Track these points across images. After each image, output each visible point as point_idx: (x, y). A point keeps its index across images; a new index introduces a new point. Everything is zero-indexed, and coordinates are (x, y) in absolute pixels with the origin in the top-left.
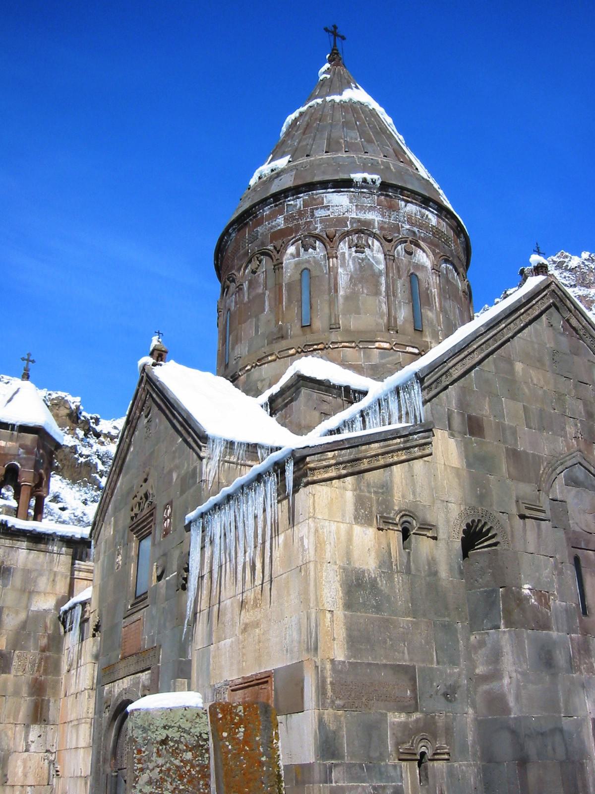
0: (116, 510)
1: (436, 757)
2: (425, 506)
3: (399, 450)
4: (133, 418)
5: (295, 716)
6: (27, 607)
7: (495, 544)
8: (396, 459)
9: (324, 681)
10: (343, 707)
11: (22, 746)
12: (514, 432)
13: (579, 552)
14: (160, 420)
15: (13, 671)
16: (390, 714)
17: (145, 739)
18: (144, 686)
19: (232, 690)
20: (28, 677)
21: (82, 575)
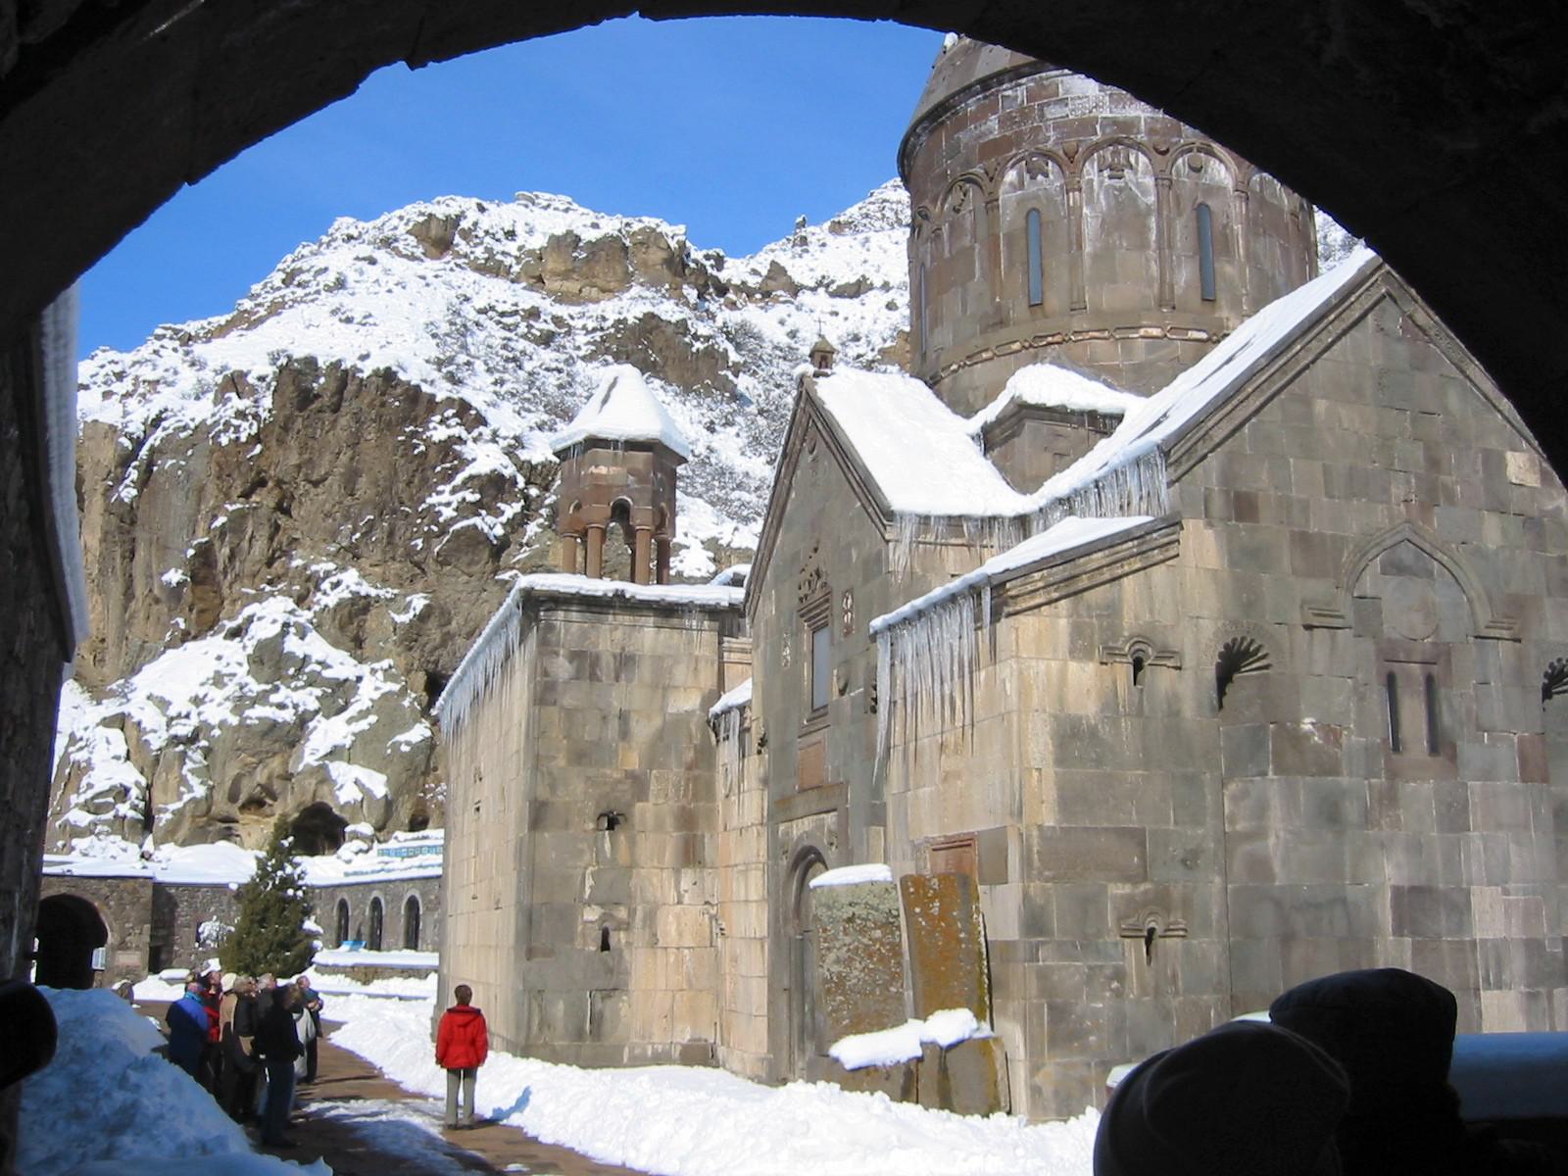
0: (777, 579)
2: (1165, 627)
3: (1132, 556)
4: (792, 449)
5: (1000, 888)
6: (663, 709)
7: (1266, 667)
8: (1127, 569)
9: (1029, 850)
11: (672, 896)
12: (1305, 507)
13: (1396, 667)
14: (830, 463)
17: (830, 917)
18: (830, 831)
19: (934, 850)
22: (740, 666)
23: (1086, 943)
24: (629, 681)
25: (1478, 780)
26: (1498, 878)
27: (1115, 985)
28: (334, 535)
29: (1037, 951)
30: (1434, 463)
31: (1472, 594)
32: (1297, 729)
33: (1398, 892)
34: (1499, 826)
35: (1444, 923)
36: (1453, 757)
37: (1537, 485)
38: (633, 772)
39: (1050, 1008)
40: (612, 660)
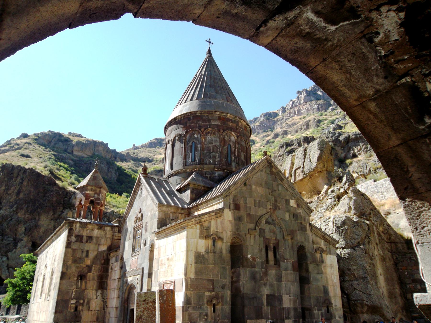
6: (98, 250)
11: (95, 297)
12: (250, 208)
15: (92, 272)
20: (97, 273)
21: (116, 238)
23: (199, 307)
24: (90, 243)
26: (288, 294)
27: (205, 317)
28: (12, 207)
32: (247, 257)
33: (267, 296)
34: (288, 281)
35: (277, 303)
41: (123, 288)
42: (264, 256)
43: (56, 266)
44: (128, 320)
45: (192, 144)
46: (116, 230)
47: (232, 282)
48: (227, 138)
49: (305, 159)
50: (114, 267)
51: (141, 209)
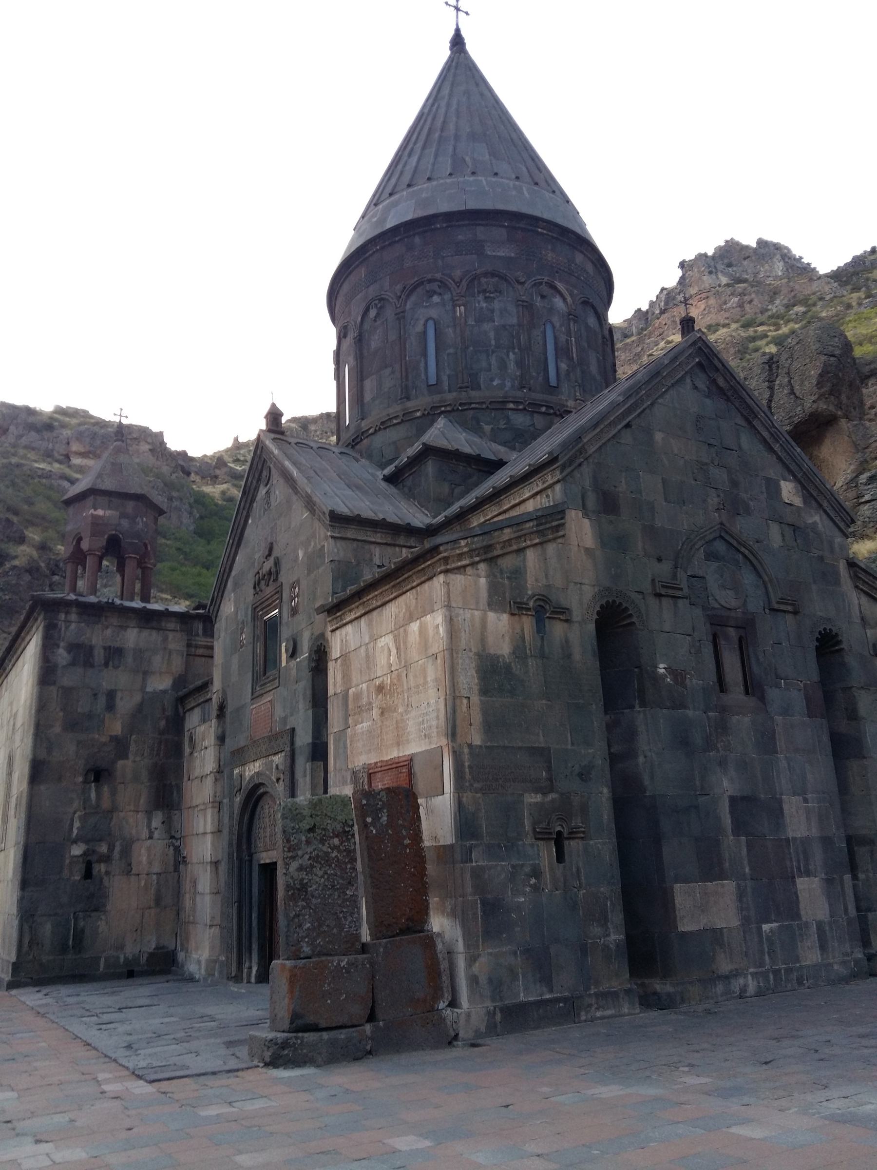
0: (236, 585)
1: (573, 836)
3: (532, 533)
6: (143, 689)
8: (529, 543)
9: (463, 765)
10: (481, 789)
11: (145, 833)
15: (131, 757)
16: (526, 795)
17: (293, 828)
21: (200, 651)
22: (203, 659)
24: (116, 667)
25: (781, 715)
26: (801, 792)
27: (533, 881)
29: (471, 853)
30: (735, 484)
31: (767, 579)
33: (732, 799)
36: (762, 698)
37: (801, 505)
38: (116, 736)
39: (484, 903)
40: (102, 651)
41: (231, 801)
42: (712, 666)
43: (18, 743)
44: (255, 899)
45: (425, 325)
46: (199, 627)
47: (614, 759)
48: (538, 302)
49: (771, 388)
50: (197, 737)
51: (272, 544)
